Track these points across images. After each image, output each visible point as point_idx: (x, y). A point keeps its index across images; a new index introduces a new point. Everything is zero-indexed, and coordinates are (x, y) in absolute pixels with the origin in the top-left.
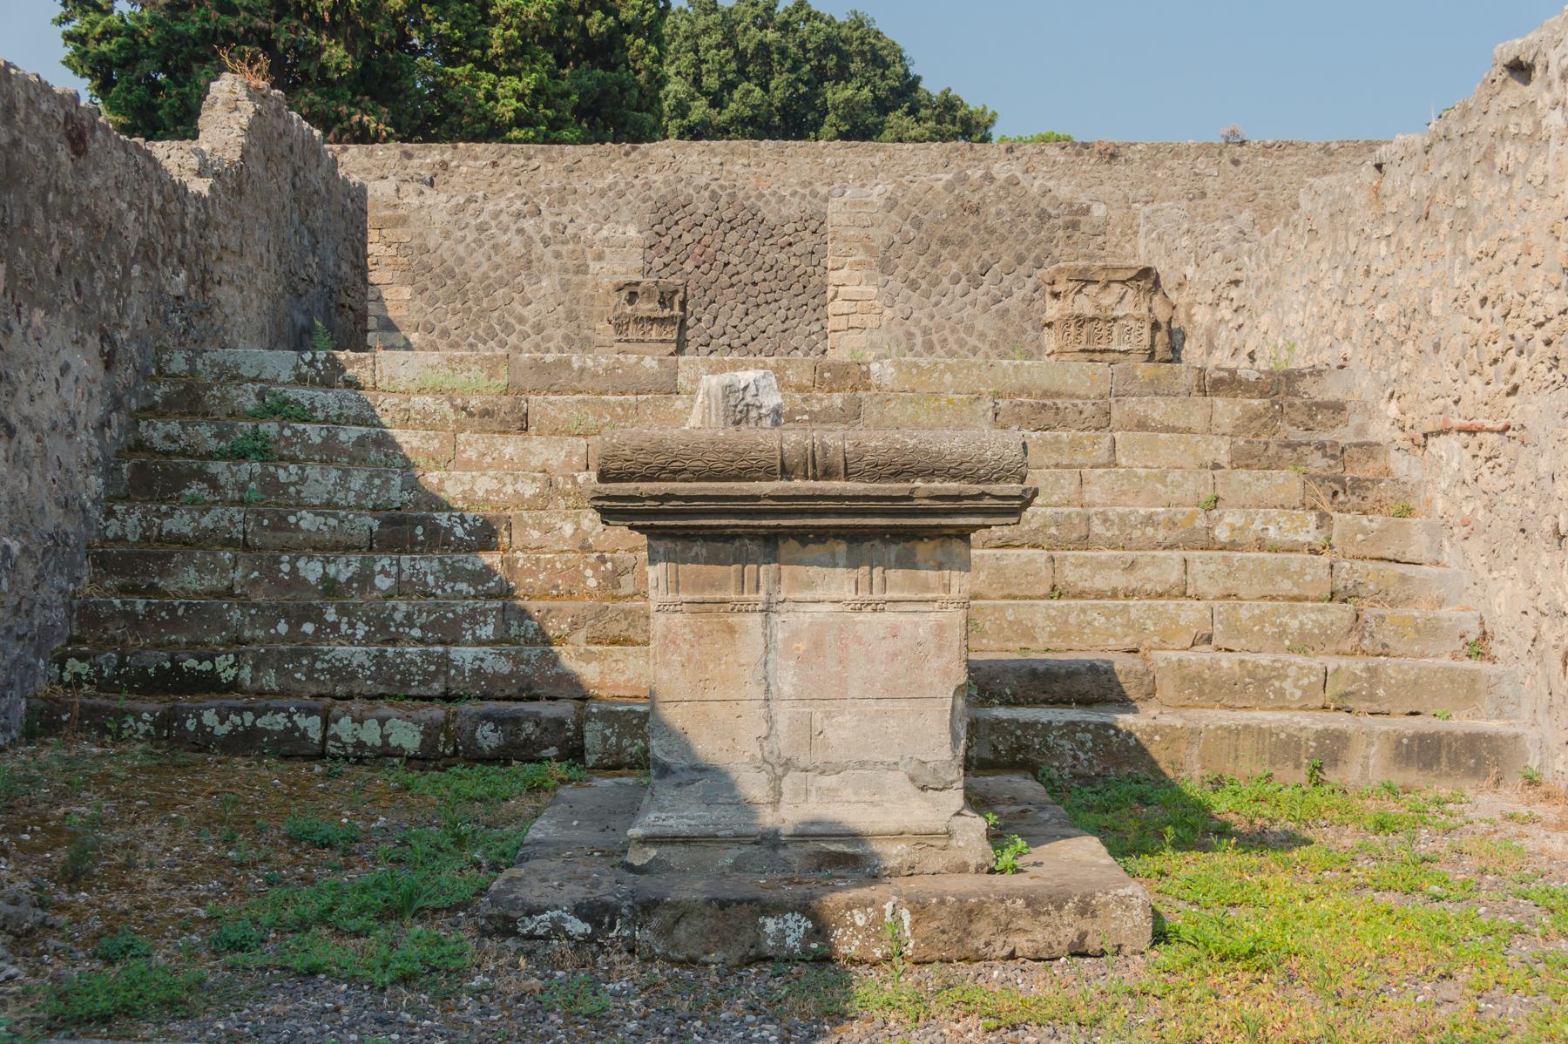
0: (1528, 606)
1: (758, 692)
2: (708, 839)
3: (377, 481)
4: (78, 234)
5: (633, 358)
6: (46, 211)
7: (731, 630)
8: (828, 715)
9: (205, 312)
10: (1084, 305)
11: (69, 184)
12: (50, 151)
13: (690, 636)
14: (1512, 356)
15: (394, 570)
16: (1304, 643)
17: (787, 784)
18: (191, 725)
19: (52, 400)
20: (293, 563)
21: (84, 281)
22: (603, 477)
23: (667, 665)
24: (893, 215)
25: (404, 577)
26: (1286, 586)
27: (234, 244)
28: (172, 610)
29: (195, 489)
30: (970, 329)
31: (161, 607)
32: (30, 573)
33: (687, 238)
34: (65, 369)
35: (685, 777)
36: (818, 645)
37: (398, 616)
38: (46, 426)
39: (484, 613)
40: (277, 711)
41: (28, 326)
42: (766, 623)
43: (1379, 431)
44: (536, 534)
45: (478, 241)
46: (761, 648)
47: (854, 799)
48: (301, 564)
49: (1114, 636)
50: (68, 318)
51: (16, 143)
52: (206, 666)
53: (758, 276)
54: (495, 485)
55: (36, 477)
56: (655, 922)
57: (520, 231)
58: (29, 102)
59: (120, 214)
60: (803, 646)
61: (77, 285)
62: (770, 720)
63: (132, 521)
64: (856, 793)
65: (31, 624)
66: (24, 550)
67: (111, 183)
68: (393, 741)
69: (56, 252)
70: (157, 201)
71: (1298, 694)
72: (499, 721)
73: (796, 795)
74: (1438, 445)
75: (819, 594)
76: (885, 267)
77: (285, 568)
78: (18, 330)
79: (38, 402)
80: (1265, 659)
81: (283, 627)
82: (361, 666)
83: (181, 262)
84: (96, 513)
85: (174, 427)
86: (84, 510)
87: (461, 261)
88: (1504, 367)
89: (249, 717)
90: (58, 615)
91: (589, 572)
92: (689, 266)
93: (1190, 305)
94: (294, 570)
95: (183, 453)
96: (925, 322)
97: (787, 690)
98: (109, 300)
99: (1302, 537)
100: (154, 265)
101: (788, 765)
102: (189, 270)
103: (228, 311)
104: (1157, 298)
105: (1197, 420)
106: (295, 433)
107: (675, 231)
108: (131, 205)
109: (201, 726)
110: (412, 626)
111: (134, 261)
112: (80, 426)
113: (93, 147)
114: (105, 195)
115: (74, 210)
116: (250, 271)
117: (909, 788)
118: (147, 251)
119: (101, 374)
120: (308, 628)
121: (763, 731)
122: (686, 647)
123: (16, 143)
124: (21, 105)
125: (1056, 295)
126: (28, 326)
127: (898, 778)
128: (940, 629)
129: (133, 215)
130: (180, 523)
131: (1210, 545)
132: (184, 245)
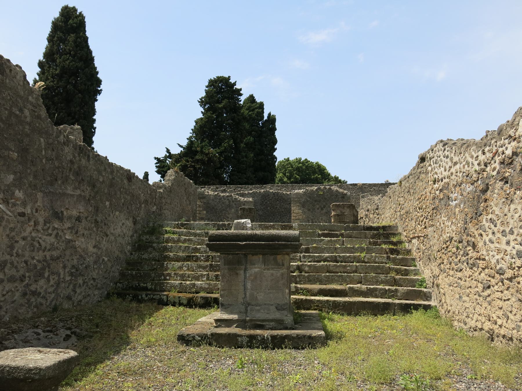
0: (431, 275)
1: (242, 288)
7: (237, 274)
8: (258, 293)
9: (160, 215)
11: (127, 187)
12: (122, 181)
14: (425, 220)
17: (249, 308)
18: (140, 297)
19: (119, 230)
21: (129, 207)
22: (210, 240)
26: (379, 271)
27: (169, 202)
28: (140, 274)
29: (150, 249)
31: (138, 273)
32: (110, 265)
33: (268, 202)
34: (123, 224)
35: (227, 306)
36: (256, 277)
37: (186, 275)
38: (117, 235)
39: (204, 275)
40: (158, 295)
42: (245, 272)
43: (403, 238)
45: (220, 202)
46: (243, 278)
50: (125, 214)
51: (113, 178)
52: (145, 285)
53: (283, 210)
55: (113, 245)
57: (228, 200)
58: (117, 171)
59: (139, 194)
61: (128, 207)
62: (245, 294)
63: (136, 255)
65: (109, 276)
66: (108, 260)
69: (123, 201)
74: (414, 241)
76: (303, 206)
78: (112, 215)
79: (116, 230)
80: (372, 287)
83: (155, 204)
84: (128, 254)
85: (148, 237)
86: (125, 253)
87: (215, 206)
88: (423, 222)
89: (152, 296)
90: (117, 274)
92: (269, 208)
95: (149, 242)
97: (249, 287)
98: (136, 211)
99: (384, 261)
100: (147, 205)
101: (249, 304)
102: (157, 206)
103: (166, 215)
105: (363, 236)
107: (266, 201)
108: (142, 193)
109: (142, 298)
111: (142, 204)
112: (126, 236)
113: (133, 180)
115: (128, 193)
116: (173, 207)
117: (275, 310)
118: (146, 201)
119: (133, 226)
121: (244, 296)
122: (227, 278)
123: (113, 178)
124: (115, 171)
126: (115, 214)
127: (273, 308)
128: (282, 274)
130: (146, 256)
132: (156, 201)
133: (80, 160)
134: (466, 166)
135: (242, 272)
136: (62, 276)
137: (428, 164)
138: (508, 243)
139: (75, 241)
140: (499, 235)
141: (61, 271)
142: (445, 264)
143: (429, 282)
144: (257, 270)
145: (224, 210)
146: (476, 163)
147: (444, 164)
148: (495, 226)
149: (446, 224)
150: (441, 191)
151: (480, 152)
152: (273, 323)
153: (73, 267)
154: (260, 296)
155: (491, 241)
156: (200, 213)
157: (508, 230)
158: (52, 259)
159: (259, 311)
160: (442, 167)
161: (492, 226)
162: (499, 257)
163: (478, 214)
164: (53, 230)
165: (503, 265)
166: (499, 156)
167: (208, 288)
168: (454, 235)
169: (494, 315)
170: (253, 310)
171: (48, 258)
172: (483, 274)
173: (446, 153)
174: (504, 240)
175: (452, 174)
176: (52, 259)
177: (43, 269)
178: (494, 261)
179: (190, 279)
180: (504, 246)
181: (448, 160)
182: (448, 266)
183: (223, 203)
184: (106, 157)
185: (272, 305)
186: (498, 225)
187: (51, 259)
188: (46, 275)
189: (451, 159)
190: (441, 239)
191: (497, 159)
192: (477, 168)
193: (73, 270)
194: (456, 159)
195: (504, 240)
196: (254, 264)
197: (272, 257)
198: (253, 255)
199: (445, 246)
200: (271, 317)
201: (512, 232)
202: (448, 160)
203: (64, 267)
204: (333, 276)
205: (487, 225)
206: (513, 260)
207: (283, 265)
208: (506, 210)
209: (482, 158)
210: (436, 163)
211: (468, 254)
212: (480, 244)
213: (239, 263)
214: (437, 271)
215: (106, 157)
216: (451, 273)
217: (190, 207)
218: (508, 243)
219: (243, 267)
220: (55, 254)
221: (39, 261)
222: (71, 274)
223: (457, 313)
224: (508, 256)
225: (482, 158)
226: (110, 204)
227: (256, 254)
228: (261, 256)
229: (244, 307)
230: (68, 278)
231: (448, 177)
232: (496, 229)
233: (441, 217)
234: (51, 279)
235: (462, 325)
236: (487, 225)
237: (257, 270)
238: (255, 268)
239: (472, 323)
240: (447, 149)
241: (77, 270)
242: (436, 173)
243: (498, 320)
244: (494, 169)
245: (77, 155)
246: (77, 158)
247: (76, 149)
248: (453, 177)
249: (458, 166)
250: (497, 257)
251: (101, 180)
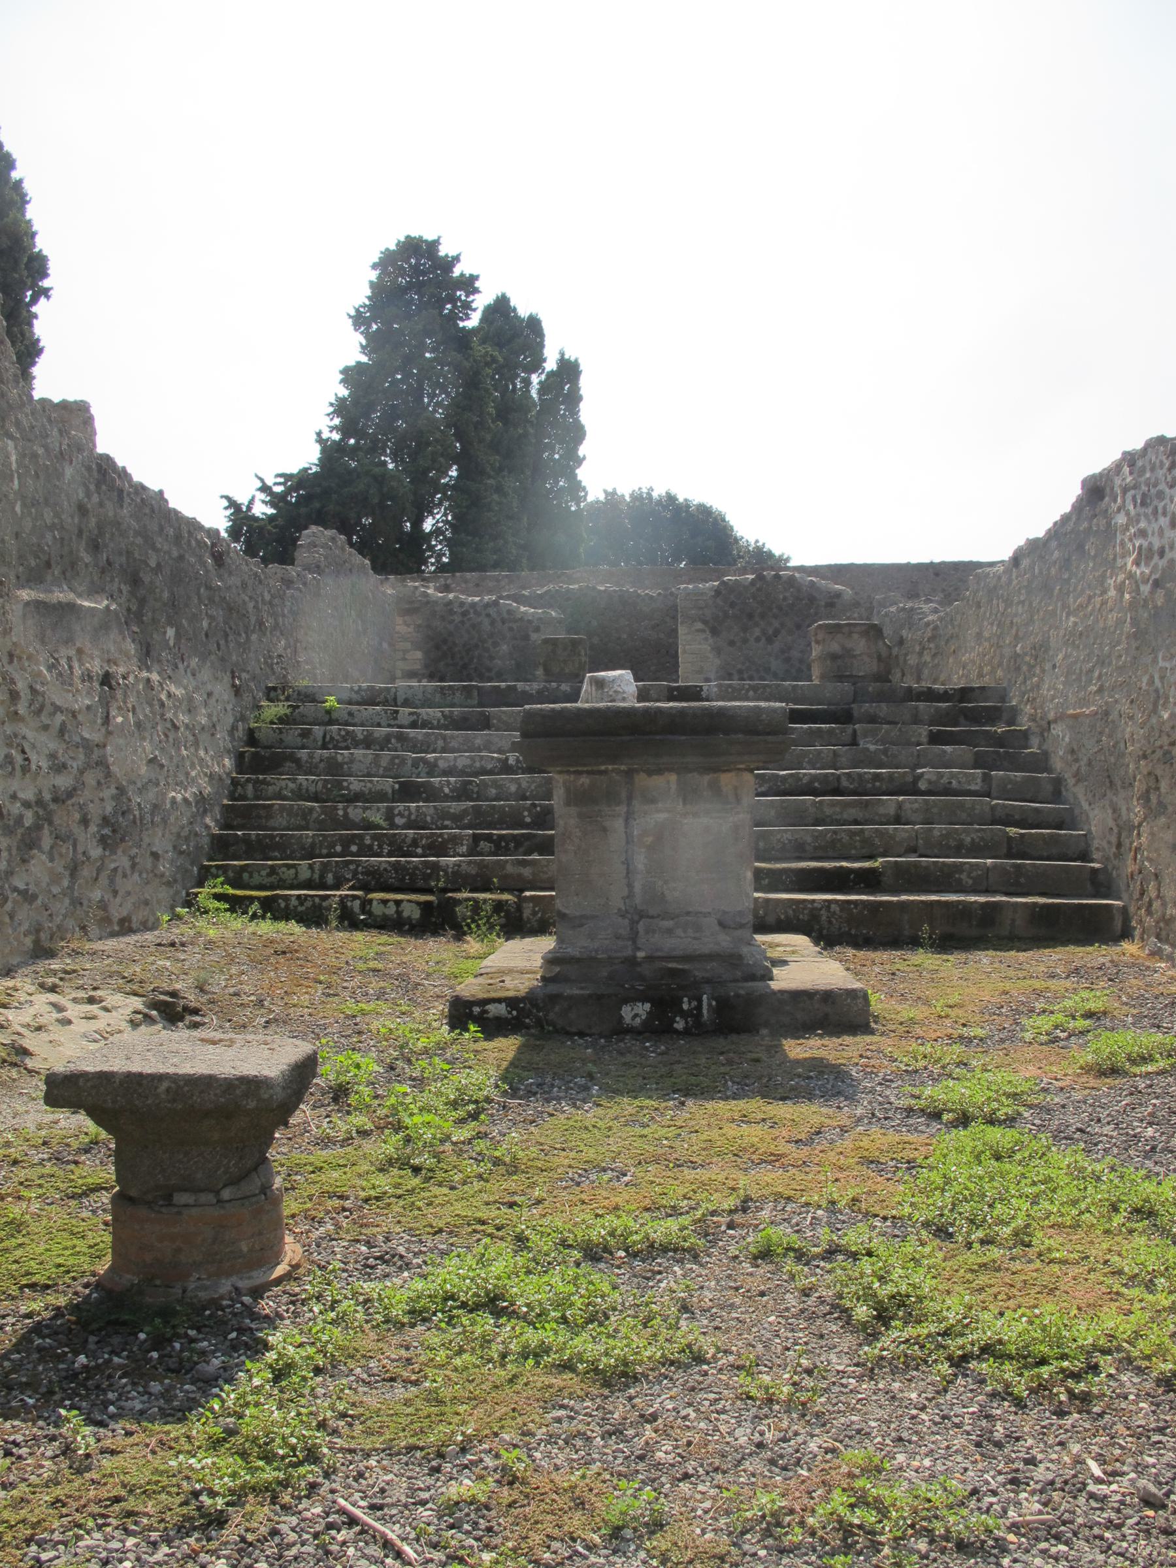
3: (397, 761)
4: (219, 614)
5: (554, 684)
6: (199, 598)
7: (605, 830)
10: (835, 647)
13: (579, 834)
15: (406, 813)
16: (976, 850)
17: (641, 927)
20: (345, 809)
21: (222, 642)
24: (719, 601)
25: (413, 817)
26: (964, 816)
34: (209, 695)
41: (188, 666)
44: (494, 791)
45: (462, 622)
47: (683, 935)
48: (350, 810)
49: (855, 848)
51: (181, 558)
54: (468, 762)
56: (557, 1009)
57: (488, 615)
58: (189, 532)
60: (650, 839)
61: (218, 645)
62: (630, 886)
64: (685, 932)
67: (239, 584)
68: (405, 914)
69: (205, 624)
70: (267, 597)
71: (970, 882)
73: (647, 932)
76: (715, 632)
77: (341, 813)
81: (338, 848)
82: (385, 869)
91: (526, 813)
93: (906, 655)
94: (346, 814)
96: (739, 666)
97: (640, 867)
99: (973, 787)
106: (348, 732)
110: (417, 847)
111: (253, 631)
114: (234, 590)
117: (717, 928)
119: (233, 700)
120: (354, 848)
121: (626, 893)
123: (181, 558)
125: (817, 642)
126: (188, 666)
129: (251, 605)
131: (917, 792)
133: (101, 504)
135: (619, 824)
136: (80, 849)
137: (1114, 507)
139: (105, 746)
141: (77, 830)
142: (1163, 790)
143: (1104, 844)
144: (662, 816)
145: (477, 646)
150: (1157, 584)
153: (105, 821)
156: (404, 659)
158: (55, 800)
160: (1164, 514)
164: (53, 714)
167: (477, 875)
170: (654, 932)
171: (47, 796)
176: (55, 800)
177: (37, 827)
179: (419, 851)
183: (474, 626)
184: (161, 492)
187: (36, 803)
188: (47, 842)
190: (1154, 720)
193: (106, 831)
196: (653, 801)
197: (706, 779)
198: (650, 773)
203: (85, 821)
204: (835, 832)
210: (1143, 504)
213: (611, 797)
215: (161, 492)
219: (622, 809)
220: (63, 782)
221: (27, 805)
222: (103, 841)
226: (178, 636)
227: (659, 771)
228: (673, 778)
230: (96, 852)
233: (1155, 661)
234: (56, 856)
237: (662, 816)
238: (658, 811)
241: (114, 831)
242: (1143, 533)
245: (92, 487)
246: (95, 498)
247: (89, 469)
251: (153, 564)
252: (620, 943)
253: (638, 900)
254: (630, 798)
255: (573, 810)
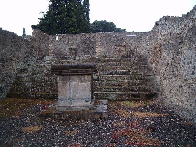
1: (69, 91)
2: (64, 107)
7: (66, 85)
8: (76, 94)
10: (118, 49)
16: (138, 84)
17: (72, 101)
23: (60, 89)
30: (111, 52)
36: (75, 86)
60: (73, 87)
72: (53, 94)
74: (153, 63)
75: (75, 81)
97: (72, 91)
104: (126, 48)
128: (88, 84)
134: (174, 30)
135: (68, 84)
138: (189, 68)
140: (186, 64)
146: (178, 29)
147: (166, 28)
148: (185, 59)
149: (166, 57)
151: (179, 24)
152: (84, 107)
154: (77, 95)
155: (183, 66)
157: (189, 62)
159: (77, 102)
161: (184, 59)
162: (185, 74)
163: (178, 53)
165: (187, 77)
166: (187, 27)
168: (169, 62)
169: (183, 100)
172: (179, 81)
173: (167, 23)
174: (188, 66)
175: (168, 33)
178: (184, 75)
180: (188, 69)
181: (167, 26)
182: (166, 77)
185: (82, 99)
186: (186, 59)
189: (168, 26)
191: (186, 28)
192: (178, 32)
194: (170, 26)
195: (188, 66)
196: (74, 80)
197: (83, 76)
199: (165, 67)
200: (83, 104)
201: (191, 63)
202: (167, 26)
205: (182, 59)
206: (191, 76)
207: (88, 80)
208: (189, 53)
209: (180, 27)
211: (174, 72)
212: (179, 67)
213: (67, 80)
214: (162, 79)
216: (168, 80)
217: (46, 47)
218: (189, 68)
223: (169, 98)
224: (189, 74)
225: (180, 27)
228: (77, 76)
229: (70, 100)
231: (167, 34)
232: (185, 61)
235: (171, 103)
236: (182, 59)
238: (74, 82)
239: (174, 103)
240: (166, 21)
243: (184, 102)
244: (185, 32)
248: (169, 35)
249: (171, 30)
250: (185, 74)
252: (69, 104)
253: (71, 97)
254: (70, 80)
255: (61, 82)
